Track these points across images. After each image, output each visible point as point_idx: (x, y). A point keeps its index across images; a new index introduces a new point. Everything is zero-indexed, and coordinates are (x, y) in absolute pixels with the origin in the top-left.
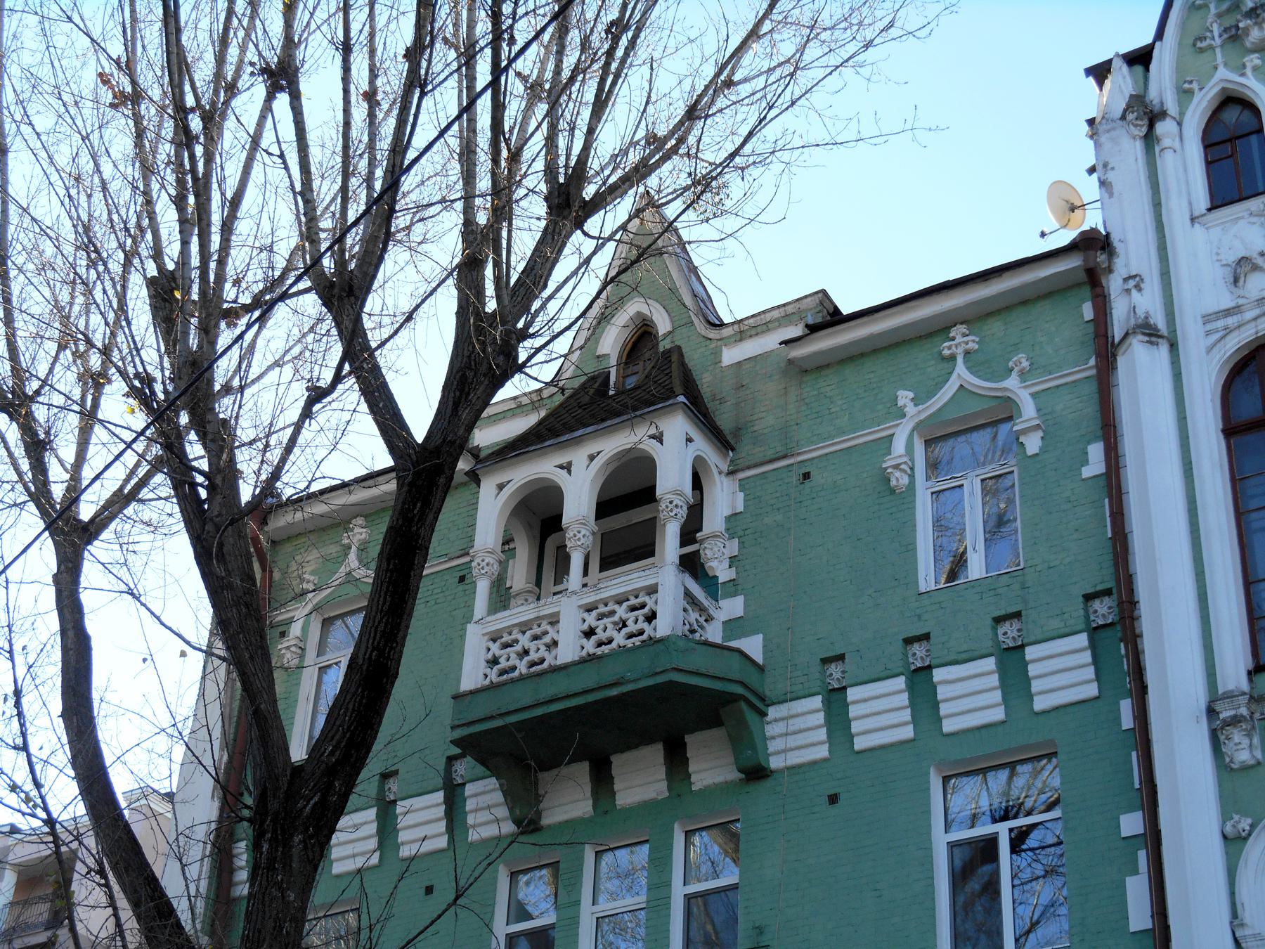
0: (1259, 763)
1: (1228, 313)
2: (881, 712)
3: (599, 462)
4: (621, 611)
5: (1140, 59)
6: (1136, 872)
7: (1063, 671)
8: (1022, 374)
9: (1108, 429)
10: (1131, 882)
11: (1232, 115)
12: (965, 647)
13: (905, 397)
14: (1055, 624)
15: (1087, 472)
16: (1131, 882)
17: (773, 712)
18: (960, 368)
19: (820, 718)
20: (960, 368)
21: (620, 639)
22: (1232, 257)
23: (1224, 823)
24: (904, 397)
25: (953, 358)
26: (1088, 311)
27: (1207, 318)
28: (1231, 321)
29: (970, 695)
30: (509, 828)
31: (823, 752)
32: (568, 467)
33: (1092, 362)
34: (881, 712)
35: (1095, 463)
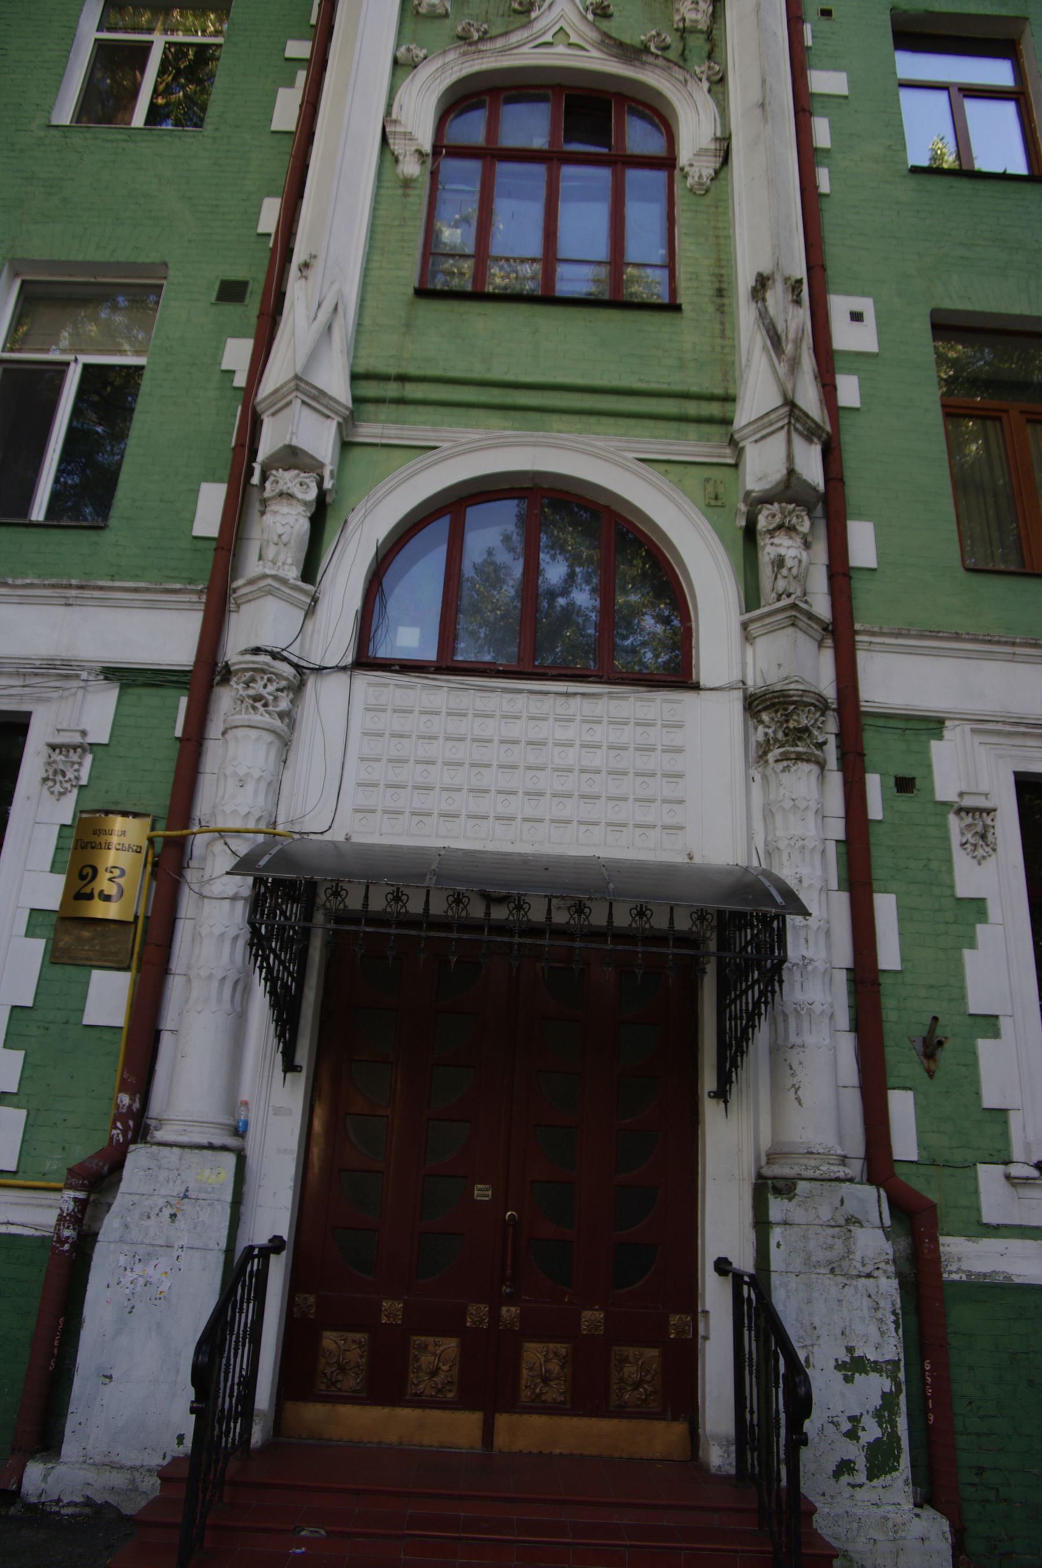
0: (446, 15)
6: (291, 84)
10: (283, 93)
16: (283, 93)
23: (398, 46)
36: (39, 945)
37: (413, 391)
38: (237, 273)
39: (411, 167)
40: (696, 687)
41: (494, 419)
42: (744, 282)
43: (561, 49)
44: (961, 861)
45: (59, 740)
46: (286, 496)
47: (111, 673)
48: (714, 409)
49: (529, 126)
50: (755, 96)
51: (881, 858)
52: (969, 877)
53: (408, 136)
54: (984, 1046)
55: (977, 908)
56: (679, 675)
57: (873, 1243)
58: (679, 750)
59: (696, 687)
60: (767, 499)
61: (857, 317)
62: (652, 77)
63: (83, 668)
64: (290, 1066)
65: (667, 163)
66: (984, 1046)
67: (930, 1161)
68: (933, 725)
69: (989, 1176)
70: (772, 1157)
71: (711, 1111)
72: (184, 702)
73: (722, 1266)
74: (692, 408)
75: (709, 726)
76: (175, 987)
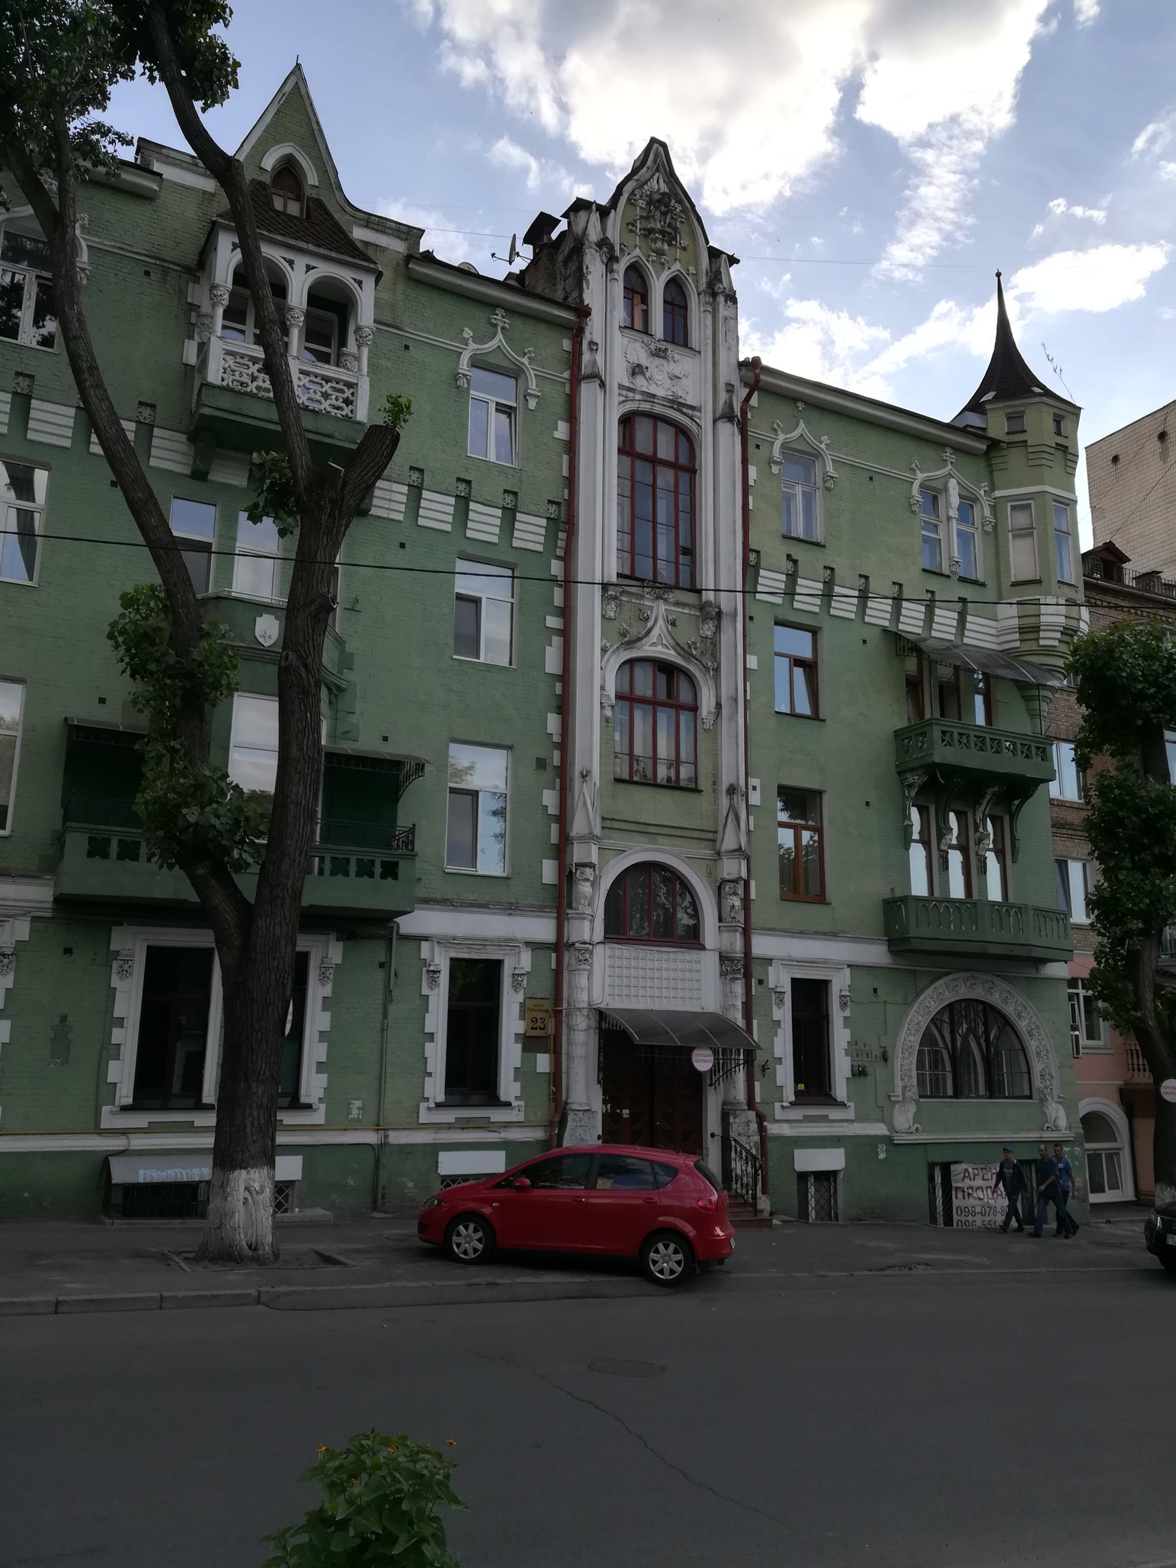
1: (629, 389)
2: (437, 510)
3: (313, 276)
4: (327, 387)
5: (604, 212)
7: (531, 531)
8: (529, 358)
9: (572, 418)
11: (634, 276)
12: (489, 498)
13: (468, 333)
14: (533, 508)
15: (557, 435)
17: (379, 484)
18: (500, 336)
19: (404, 499)
20: (500, 336)
21: (325, 405)
22: (634, 360)
24: (468, 333)
25: (495, 326)
26: (567, 344)
27: (621, 387)
28: (630, 394)
29: (484, 523)
30: (187, 471)
31: (400, 517)
32: (291, 263)
33: (566, 375)
34: (437, 510)
35: (561, 431)
36: (519, 1046)
37: (615, 825)
38: (542, 755)
39: (608, 713)
40: (703, 948)
41: (641, 838)
42: (724, 786)
43: (660, 648)
44: (774, 1007)
45: (517, 972)
46: (587, 880)
47: (528, 944)
48: (710, 836)
49: (644, 683)
50: (732, 693)
51: (755, 1008)
52: (777, 1014)
53: (608, 696)
54: (778, 1067)
55: (778, 1023)
56: (692, 939)
57: (754, 1126)
58: (699, 971)
59: (703, 948)
60: (729, 881)
61: (754, 788)
62: (693, 668)
63: (516, 940)
64: (599, 1083)
65: (694, 709)
66: (778, 1067)
67: (763, 1102)
68: (769, 961)
69: (777, 1105)
70: (724, 1103)
71: (710, 1090)
72: (554, 955)
73: (713, 1135)
74: (704, 835)
75: (708, 962)
76: (564, 1057)
